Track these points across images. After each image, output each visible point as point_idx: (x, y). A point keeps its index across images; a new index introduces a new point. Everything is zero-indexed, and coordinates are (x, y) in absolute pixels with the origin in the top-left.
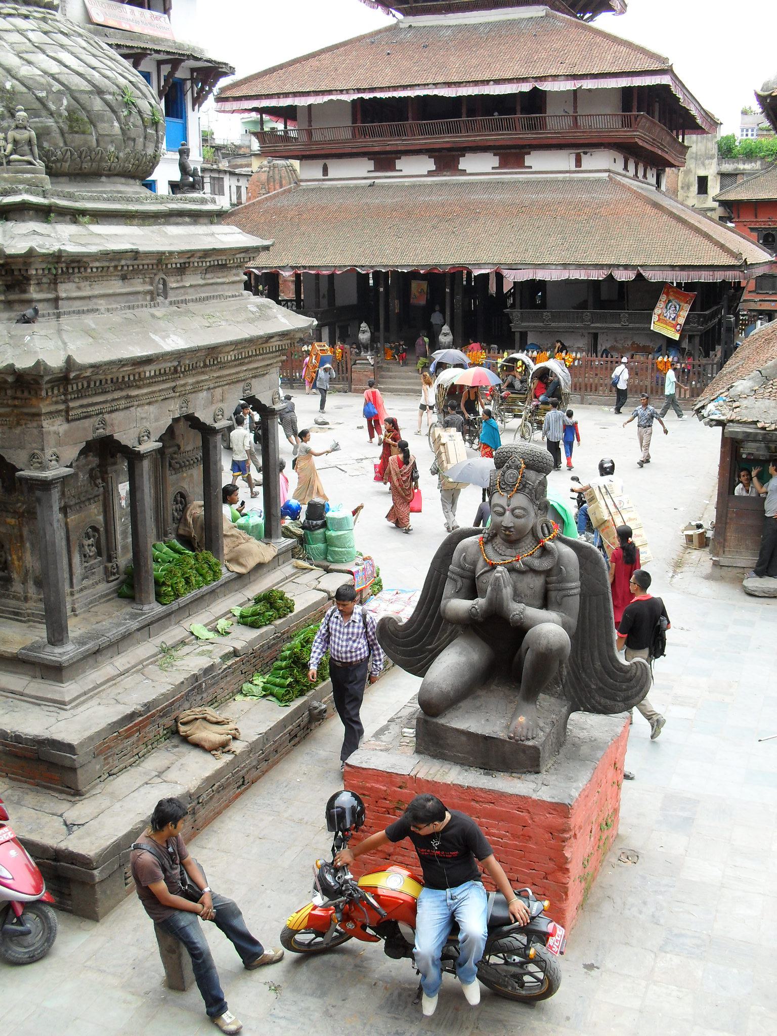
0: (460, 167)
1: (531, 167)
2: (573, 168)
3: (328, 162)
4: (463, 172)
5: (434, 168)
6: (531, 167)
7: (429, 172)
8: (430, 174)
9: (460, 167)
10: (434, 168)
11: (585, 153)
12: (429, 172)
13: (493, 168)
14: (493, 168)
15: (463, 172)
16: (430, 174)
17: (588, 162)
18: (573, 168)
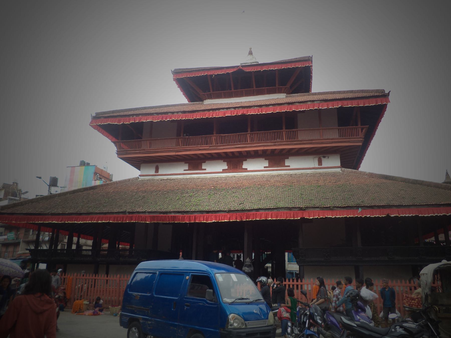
0: (244, 167)
1: (289, 166)
2: (317, 166)
3: (159, 164)
4: (246, 170)
5: (226, 168)
6: (289, 166)
7: (223, 170)
8: (224, 171)
9: (244, 167)
10: (226, 168)
11: (324, 157)
12: (223, 170)
13: (265, 167)
14: (265, 167)
15: (246, 170)
16: (224, 171)
17: (326, 163)
18: (317, 166)
